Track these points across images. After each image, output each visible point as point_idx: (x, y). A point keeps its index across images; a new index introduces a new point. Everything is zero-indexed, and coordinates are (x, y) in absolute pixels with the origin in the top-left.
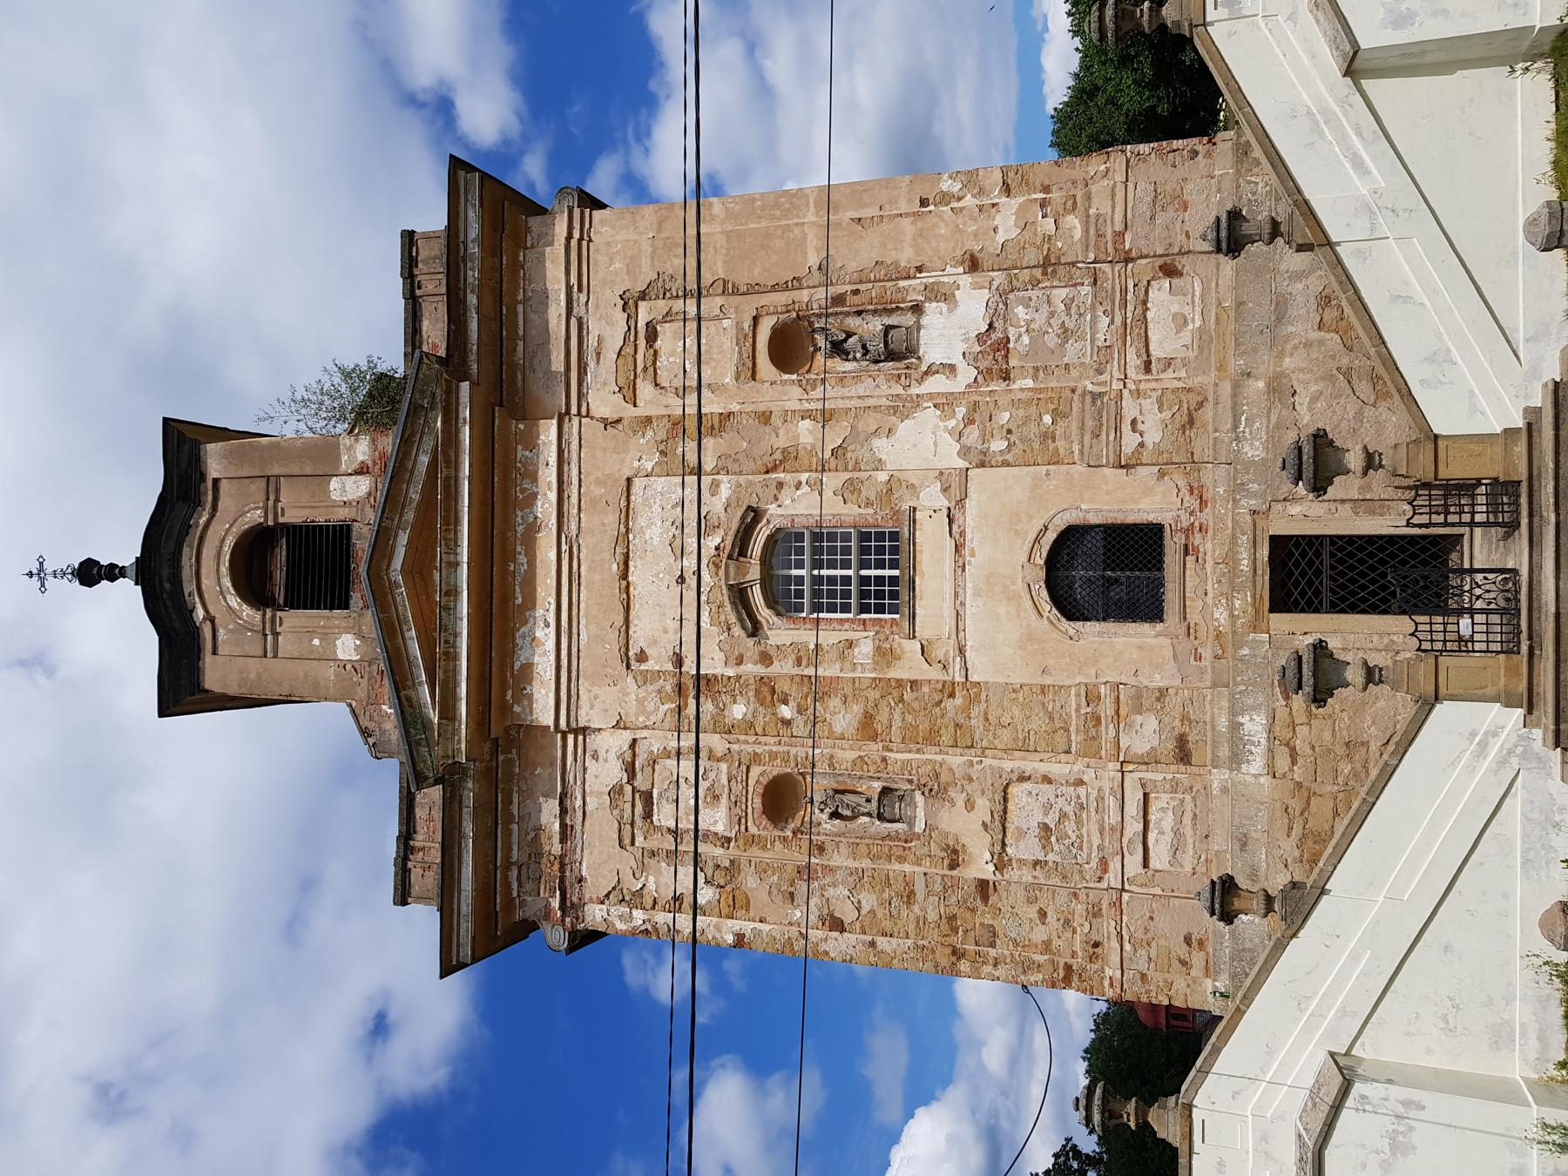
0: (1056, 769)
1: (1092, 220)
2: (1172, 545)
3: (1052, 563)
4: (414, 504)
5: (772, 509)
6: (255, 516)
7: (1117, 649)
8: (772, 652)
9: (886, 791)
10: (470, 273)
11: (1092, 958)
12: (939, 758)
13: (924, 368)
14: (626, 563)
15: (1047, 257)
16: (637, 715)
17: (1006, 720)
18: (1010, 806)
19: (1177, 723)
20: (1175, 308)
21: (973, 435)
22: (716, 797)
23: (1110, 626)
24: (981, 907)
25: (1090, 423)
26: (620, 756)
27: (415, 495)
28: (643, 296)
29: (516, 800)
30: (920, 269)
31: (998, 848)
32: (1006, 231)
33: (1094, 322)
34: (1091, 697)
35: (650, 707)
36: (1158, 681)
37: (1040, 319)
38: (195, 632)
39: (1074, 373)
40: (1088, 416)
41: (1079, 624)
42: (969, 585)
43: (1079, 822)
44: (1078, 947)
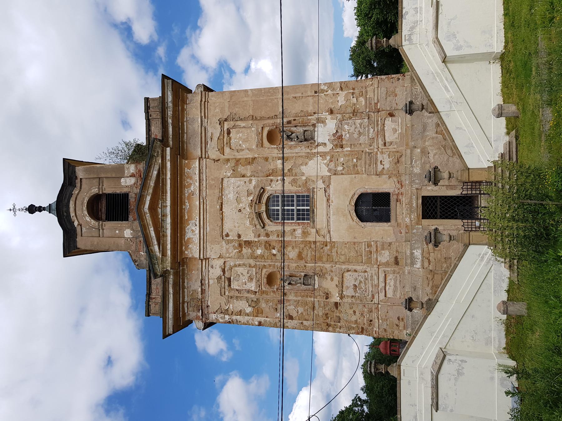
0: (358, 268)
2: (393, 199)
3: (356, 205)
4: (152, 187)
5: (268, 188)
6: (95, 191)
7: (377, 230)
8: (270, 233)
9: (305, 275)
10: (169, 112)
11: (370, 325)
12: (322, 265)
13: (316, 144)
14: (222, 205)
15: (354, 110)
16: (226, 254)
17: (343, 253)
18: (344, 280)
19: (395, 253)
20: (393, 126)
21: (332, 165)
22: (252, 279)
23: (375, 224)
24: (336, 310)
25: (368, 162)
26: (220, 267)
27: (152, 184)
28: (226, 120)
29: (186, 282)
30: (315, 113)
31: (341, 292)
32: (341, 102)
33: (369, 130)
34: (369, 245)
35: (230, 251)
36: (389, 240)
37: (352, 129)
38: (74, 229)
39: (363, 146)
40: (367, 159)
41: (365, 223)
42: (331, 212)
43: (365, 284)
44: (365, 322)
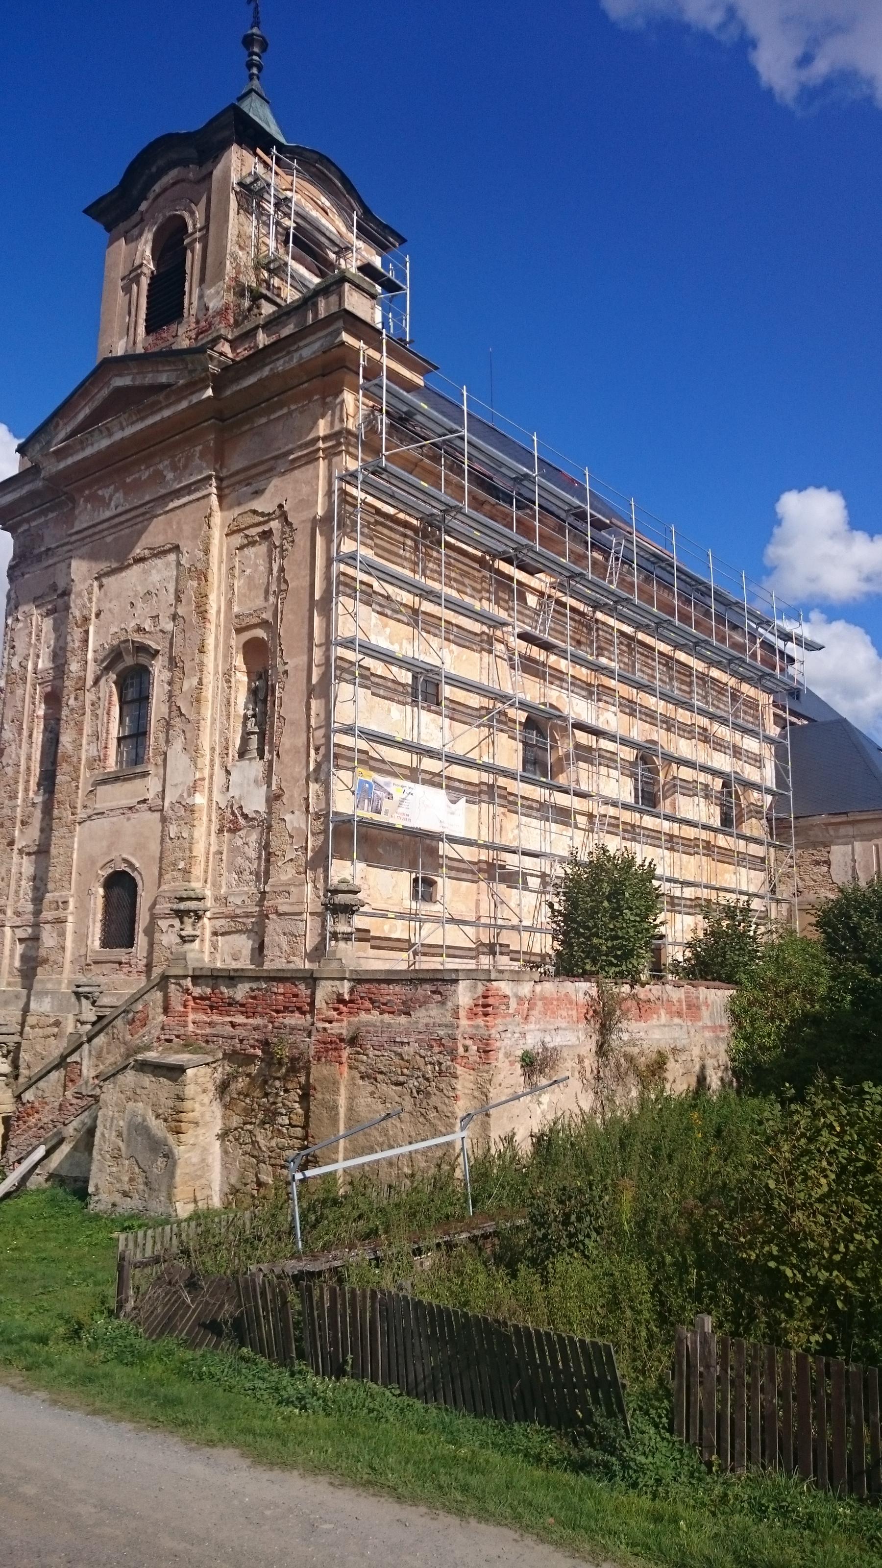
1: (287, 888)
42: (115, 819)
